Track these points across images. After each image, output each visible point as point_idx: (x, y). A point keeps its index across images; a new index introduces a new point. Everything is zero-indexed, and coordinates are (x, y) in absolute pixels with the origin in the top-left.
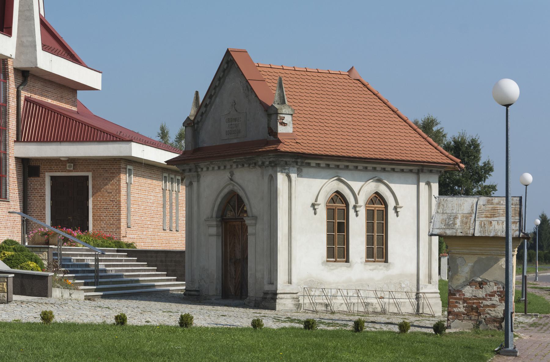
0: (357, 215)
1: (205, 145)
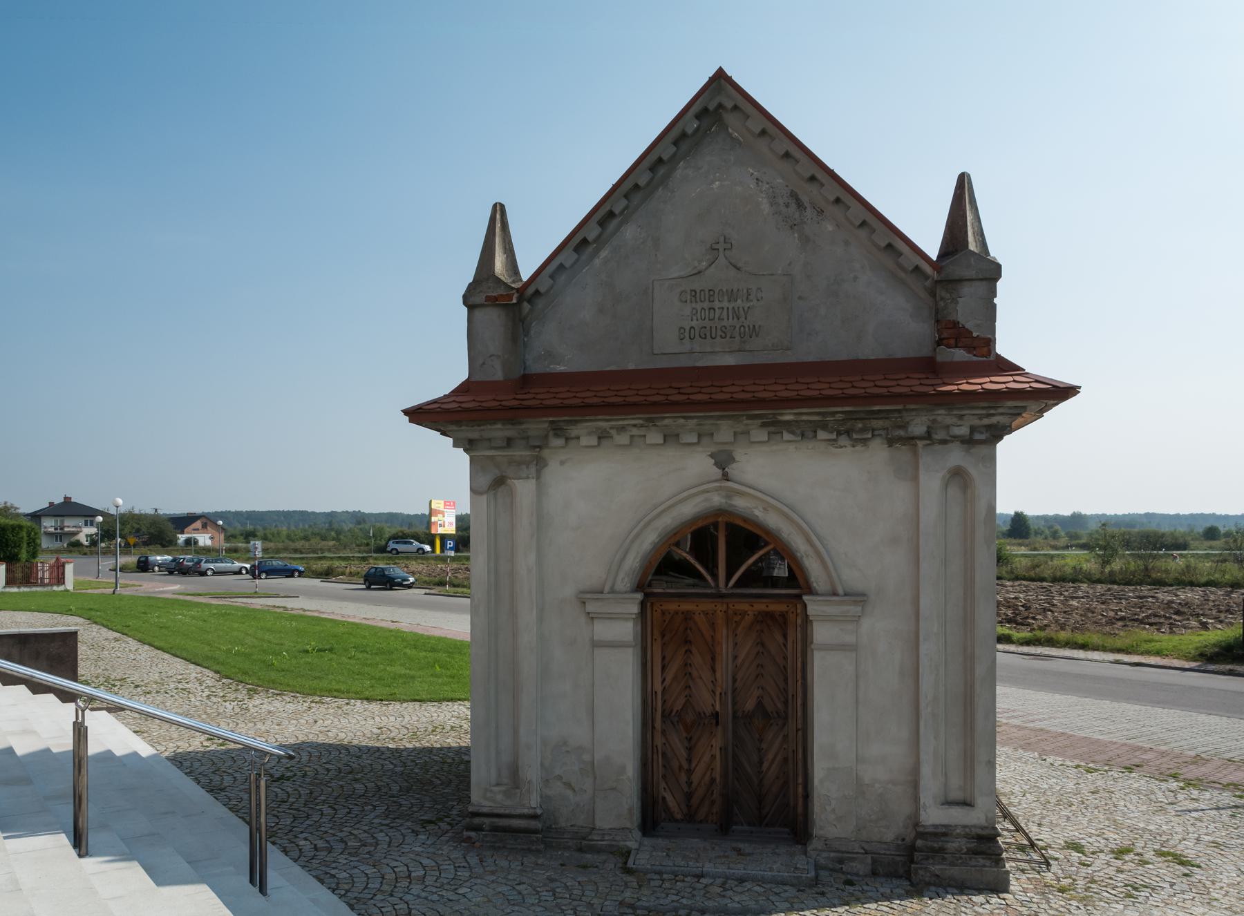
1: (561, 368)
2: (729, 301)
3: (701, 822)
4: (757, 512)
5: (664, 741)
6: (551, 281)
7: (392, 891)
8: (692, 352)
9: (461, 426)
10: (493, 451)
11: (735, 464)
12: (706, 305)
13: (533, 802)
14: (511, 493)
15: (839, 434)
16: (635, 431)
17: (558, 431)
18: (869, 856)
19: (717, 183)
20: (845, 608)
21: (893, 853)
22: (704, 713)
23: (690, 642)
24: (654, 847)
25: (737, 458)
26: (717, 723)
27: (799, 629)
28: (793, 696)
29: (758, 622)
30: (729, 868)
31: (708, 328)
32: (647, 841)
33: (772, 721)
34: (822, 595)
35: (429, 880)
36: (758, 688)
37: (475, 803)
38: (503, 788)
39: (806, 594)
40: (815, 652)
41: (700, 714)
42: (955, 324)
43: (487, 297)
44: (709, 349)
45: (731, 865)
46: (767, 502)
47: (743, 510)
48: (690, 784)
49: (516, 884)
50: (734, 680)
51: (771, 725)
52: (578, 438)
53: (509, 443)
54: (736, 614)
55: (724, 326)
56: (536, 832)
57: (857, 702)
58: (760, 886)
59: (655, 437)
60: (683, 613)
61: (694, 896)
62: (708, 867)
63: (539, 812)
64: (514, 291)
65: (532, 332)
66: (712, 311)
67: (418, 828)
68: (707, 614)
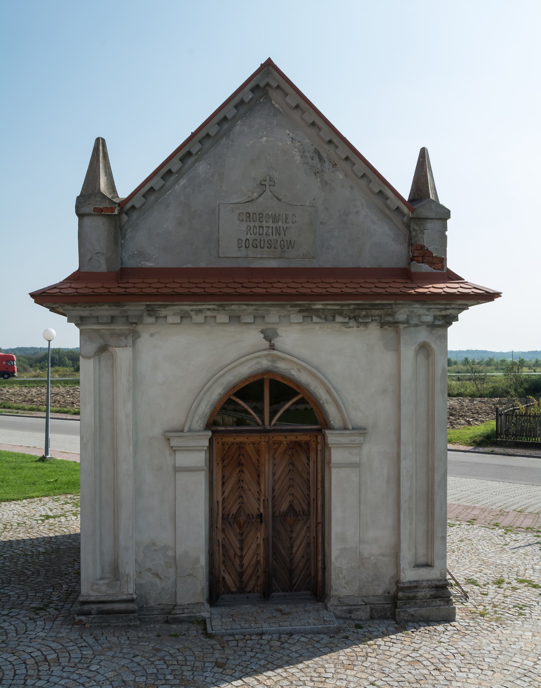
1: (150, 264)
2: (273, 222)
3: (250, 592)
4: (293, 372)
5: (224, 536)
6: (144, 200)
7: (38, 675)
8: (247, 257)
9: (75, 306)
10: (100, 326)
11: (278, 338)
12: (257, 224)
13: (130, 590)
14: (113, 358)
15: (350, 319)
16: (209, 313)
17: (151, 311)
18: (368, 607)
19: (265, 138)
20: (354, 438)
21: (383, 602)
22: (252, 515)
23: (242, 464)
24: (221, 615)
25: (280, 333)
26: (261, 522)
27: (319, 453)
28: (314, 499)
29: (290, 448)
30: (280, 626)
31: (259, 241)
32: (214, 610)
33: (299, 518)
34: (337, 429)
35: (64, 661)
36: (290, 495)
37: (84, 594)
38: (106, 581)
39: (324, 428)
40: (332, 469)
41: (249, 515)
43: (94, 208)
44: (259, 256)
45: (281, 624)
46: (300, 365)
47: (284, 371)
48: (241, 566)
49: (133, 657)
50: (273, 490)
51: (299, 520)
52: (165, 317)
53: (113, 319)
54: (274, 443)
55: (270, 240)
56: (133, 612)
57: (360, 503)
58: (304, 637)
59: (223, 318)
60: (237, 444)
61: (263, 650)
62: (266, 627)
63: (135, 596)
64: (116, 205)
65: (128, 236)
66: (261, 229)
67: (33, 615)
68: (254, 444)
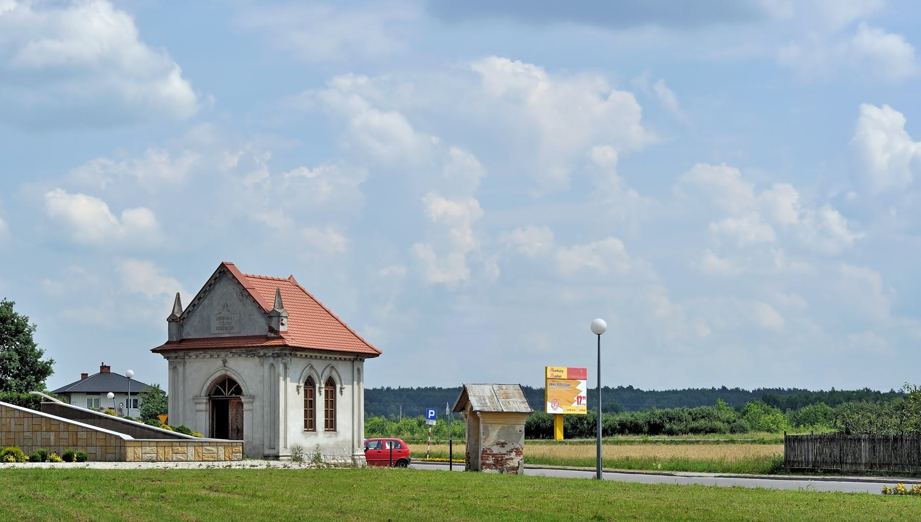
0: (320, 395)
1: (191, 337)
12: (222, 321)
42: (272, 327)
53: (176, 357)
59: (208, 356)
